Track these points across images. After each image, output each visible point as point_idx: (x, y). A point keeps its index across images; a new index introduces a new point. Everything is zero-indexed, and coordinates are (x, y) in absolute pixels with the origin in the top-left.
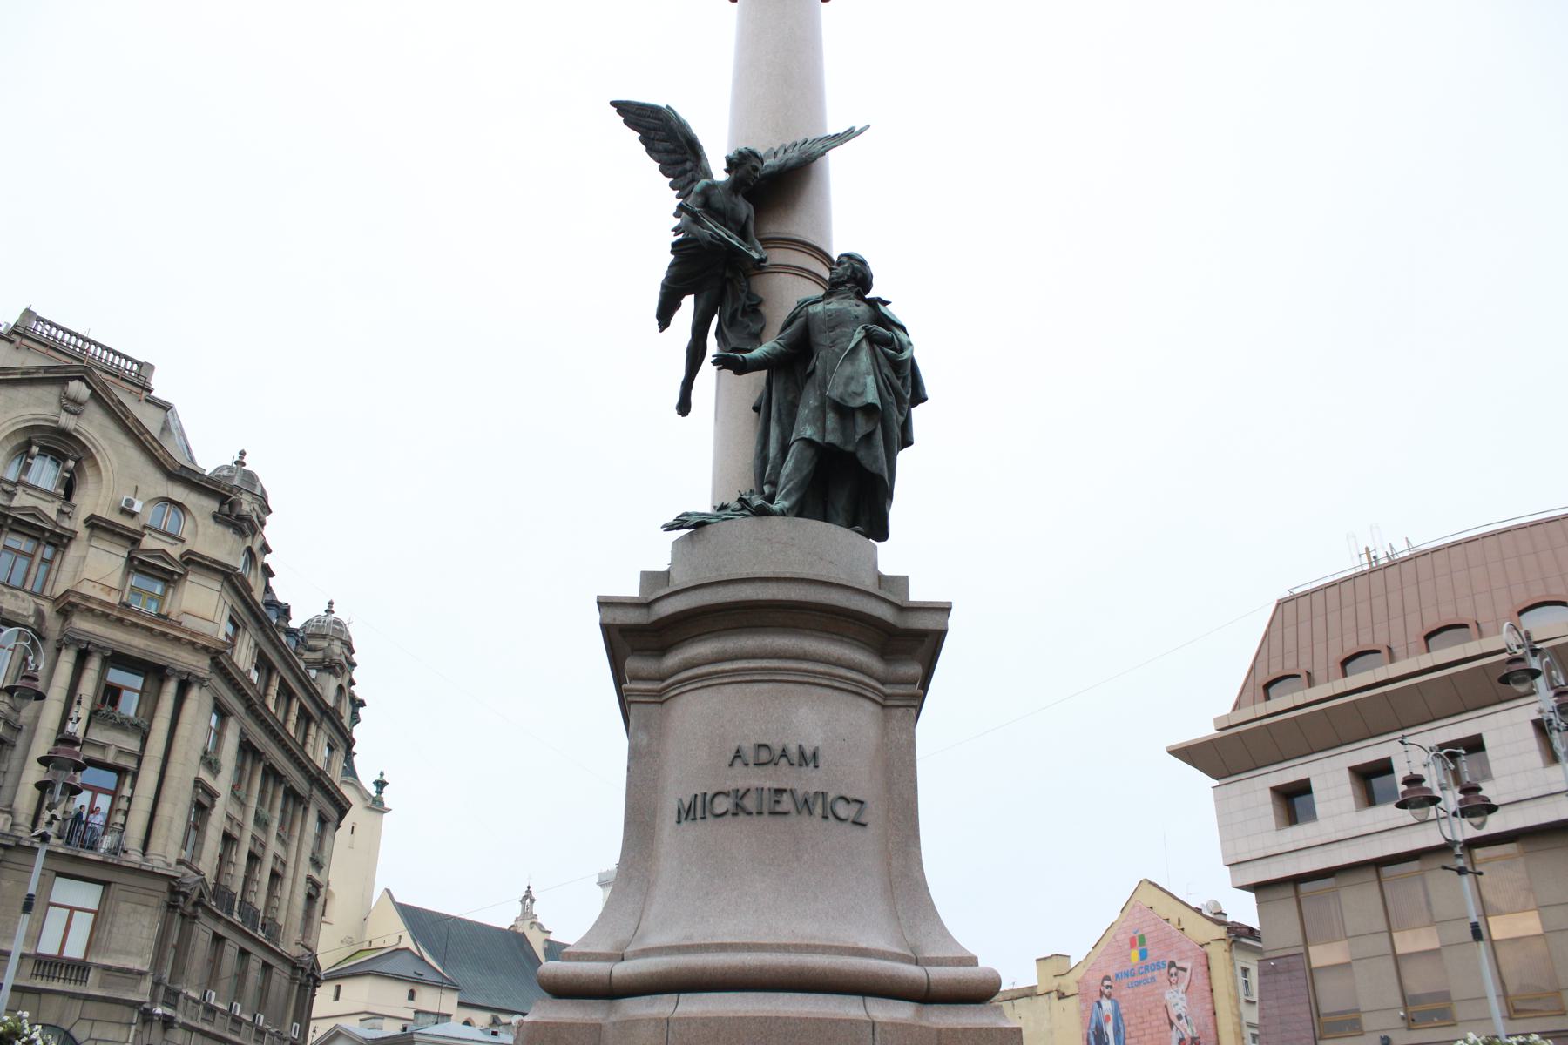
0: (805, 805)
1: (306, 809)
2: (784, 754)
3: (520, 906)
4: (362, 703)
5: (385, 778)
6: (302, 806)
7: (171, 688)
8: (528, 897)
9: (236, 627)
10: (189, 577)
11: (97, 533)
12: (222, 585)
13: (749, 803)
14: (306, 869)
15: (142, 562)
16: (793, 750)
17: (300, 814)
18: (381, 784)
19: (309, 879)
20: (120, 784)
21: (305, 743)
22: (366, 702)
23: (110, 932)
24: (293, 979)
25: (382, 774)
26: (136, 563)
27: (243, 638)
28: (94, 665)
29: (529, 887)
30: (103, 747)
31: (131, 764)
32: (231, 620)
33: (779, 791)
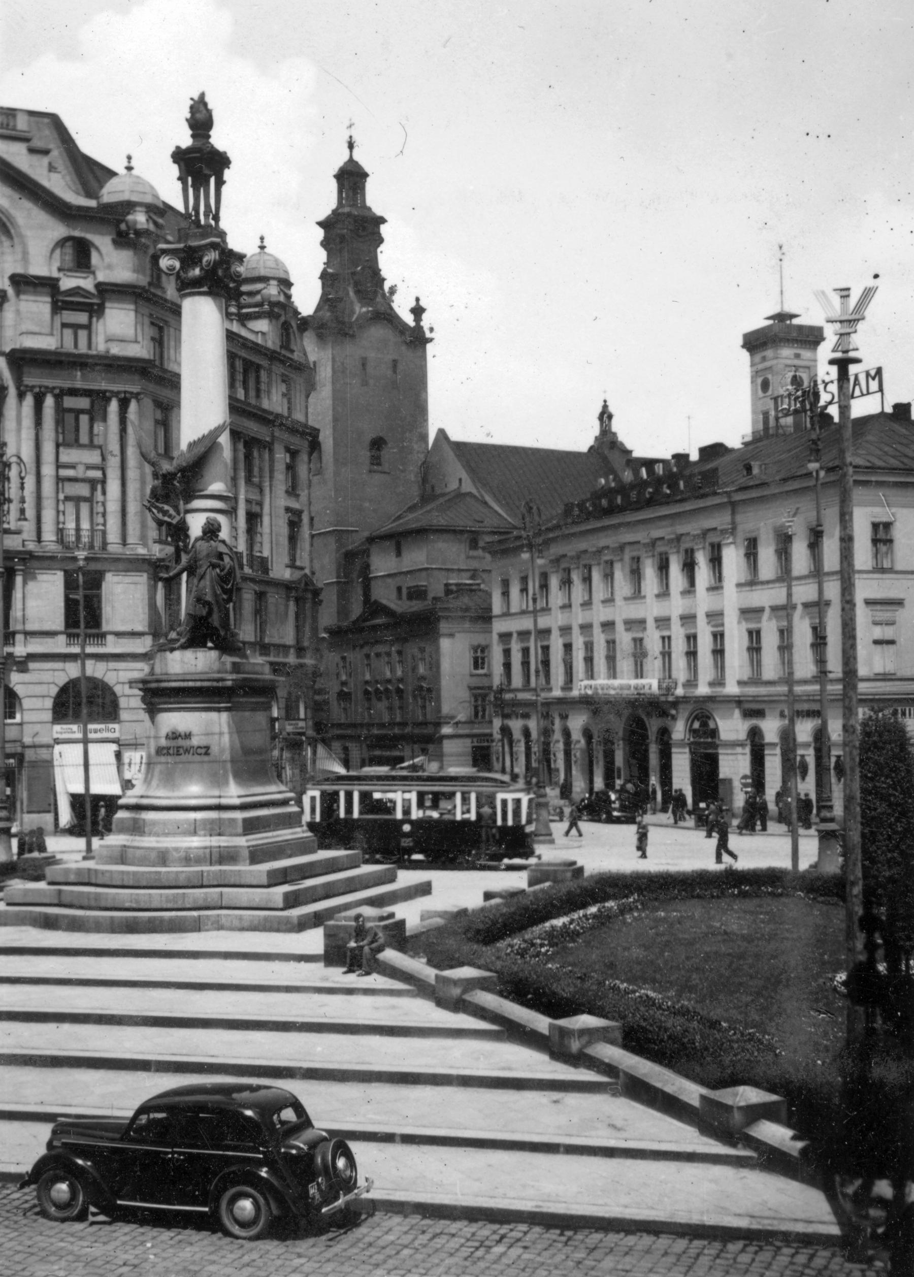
0: (187, 751)
1: (271, 451)
2: (180, 736)
3: (596, 424)
4: (382, 220)
5: (423, 303)
6: (267, 451)
7: (114, 406)
8: (605, 416)
9: (161, 329)
10: (108, 305)
11: (23, 287)
12: (136, 303)
13: (171, 751)
14: (283, 501)
15: (63, 302)
16: (183, 734)
17: (266, 456)
18: (418, 311)
19: (288, 509)
20: (93, 489)
21: (258, 391)
22: (386, 217)
23: (113, 607)
24: (288, 598)
25: (418, 300)
26: (60, 304)
27: (169, 335)
28: (49, 401)
29: (605, 401)
30: (73, 466)
31: (98, 474)
32: (152, 323)
33: (178, 747)
